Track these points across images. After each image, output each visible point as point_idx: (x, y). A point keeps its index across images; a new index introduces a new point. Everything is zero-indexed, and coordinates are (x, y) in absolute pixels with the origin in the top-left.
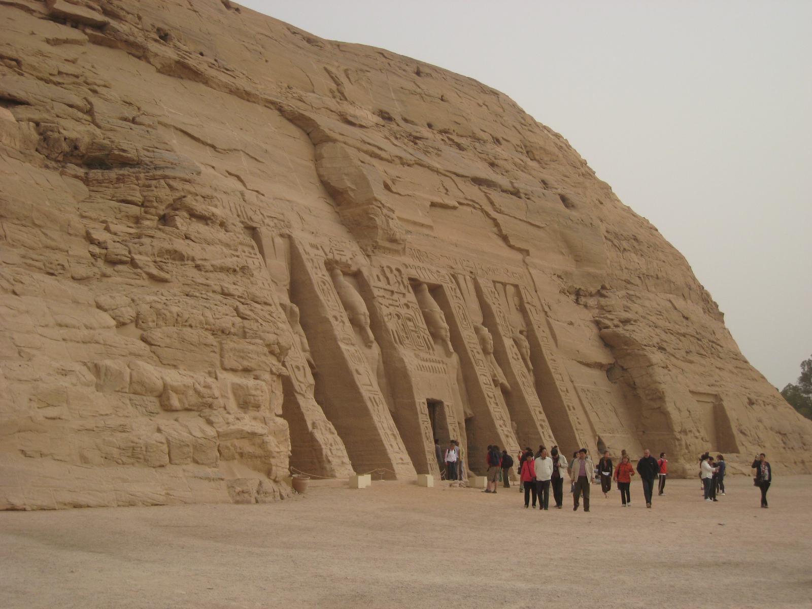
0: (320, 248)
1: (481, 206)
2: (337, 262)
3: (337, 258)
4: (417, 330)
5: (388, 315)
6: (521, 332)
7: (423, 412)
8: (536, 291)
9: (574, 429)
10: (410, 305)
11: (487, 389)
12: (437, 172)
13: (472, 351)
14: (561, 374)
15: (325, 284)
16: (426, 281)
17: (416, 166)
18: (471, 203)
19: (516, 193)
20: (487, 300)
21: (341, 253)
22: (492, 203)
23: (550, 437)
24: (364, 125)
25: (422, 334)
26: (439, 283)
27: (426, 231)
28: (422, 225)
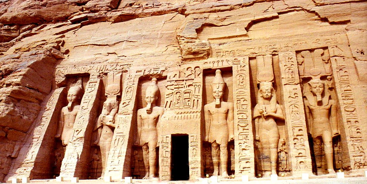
0: (143, 71)
1: (302, 8)
2: (151, 75)
3: (151, 73)
5: (171, 94)
7: (165, 142)
8: (349, 46)
9: (348, 138)
10: (194, 84)
11: (239, 122)
15: (131, 88)
16: (218, 68)
18: (293, 9)
21: (157, 69)
26: (230, 66)
27: (240, 39)
28: (236, 36)
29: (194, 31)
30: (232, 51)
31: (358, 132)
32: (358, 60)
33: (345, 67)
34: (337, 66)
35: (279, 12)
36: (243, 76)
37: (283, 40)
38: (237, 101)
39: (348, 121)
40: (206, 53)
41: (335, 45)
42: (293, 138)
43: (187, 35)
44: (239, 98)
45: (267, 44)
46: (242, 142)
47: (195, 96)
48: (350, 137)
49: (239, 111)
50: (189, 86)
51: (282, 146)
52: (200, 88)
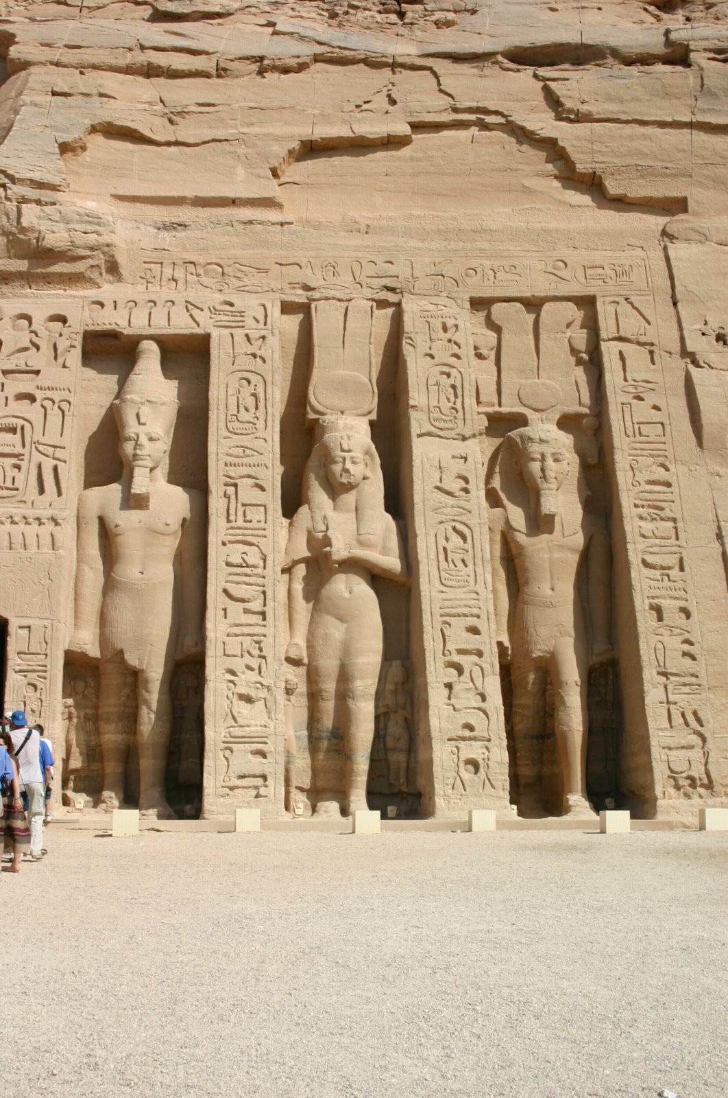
4: (26, 451)
6: (566, 422)
8: (675, 304)
9: (649, 674)
10: (39, 395)
11: (230, 578)
12: (394, 66)
13: (236, 485)
14: (674, 520)
17: (320, 66)
18: (472, 117)
19: (678, 55)
20: (406, 349)
22: (553, 101)
23: (484, 699)
24: (217, 9)
25: (37, 457)
26: (199, 331)
28: (234, 202)
29: (50, 150)
30: (209, 264)
31: (685, 654)
32: (702, 364)
33: (654, 390)
34: (625, 379)
35: (415, 119)
36: (253, 383)
37: (427, 245)
38: (226, 485)
39: (652, 607)
40: (100, 259)
41: (625, 293)
42: (441, 660)
43: (19, 168)
44: (232, 474)
45: (360, 254)
46: (238, 664)
47: (40, 447)
48: (654, 672)
49: (231, 531)
50: (21, 397)
51: (395, 692)
52: (66, 412)
